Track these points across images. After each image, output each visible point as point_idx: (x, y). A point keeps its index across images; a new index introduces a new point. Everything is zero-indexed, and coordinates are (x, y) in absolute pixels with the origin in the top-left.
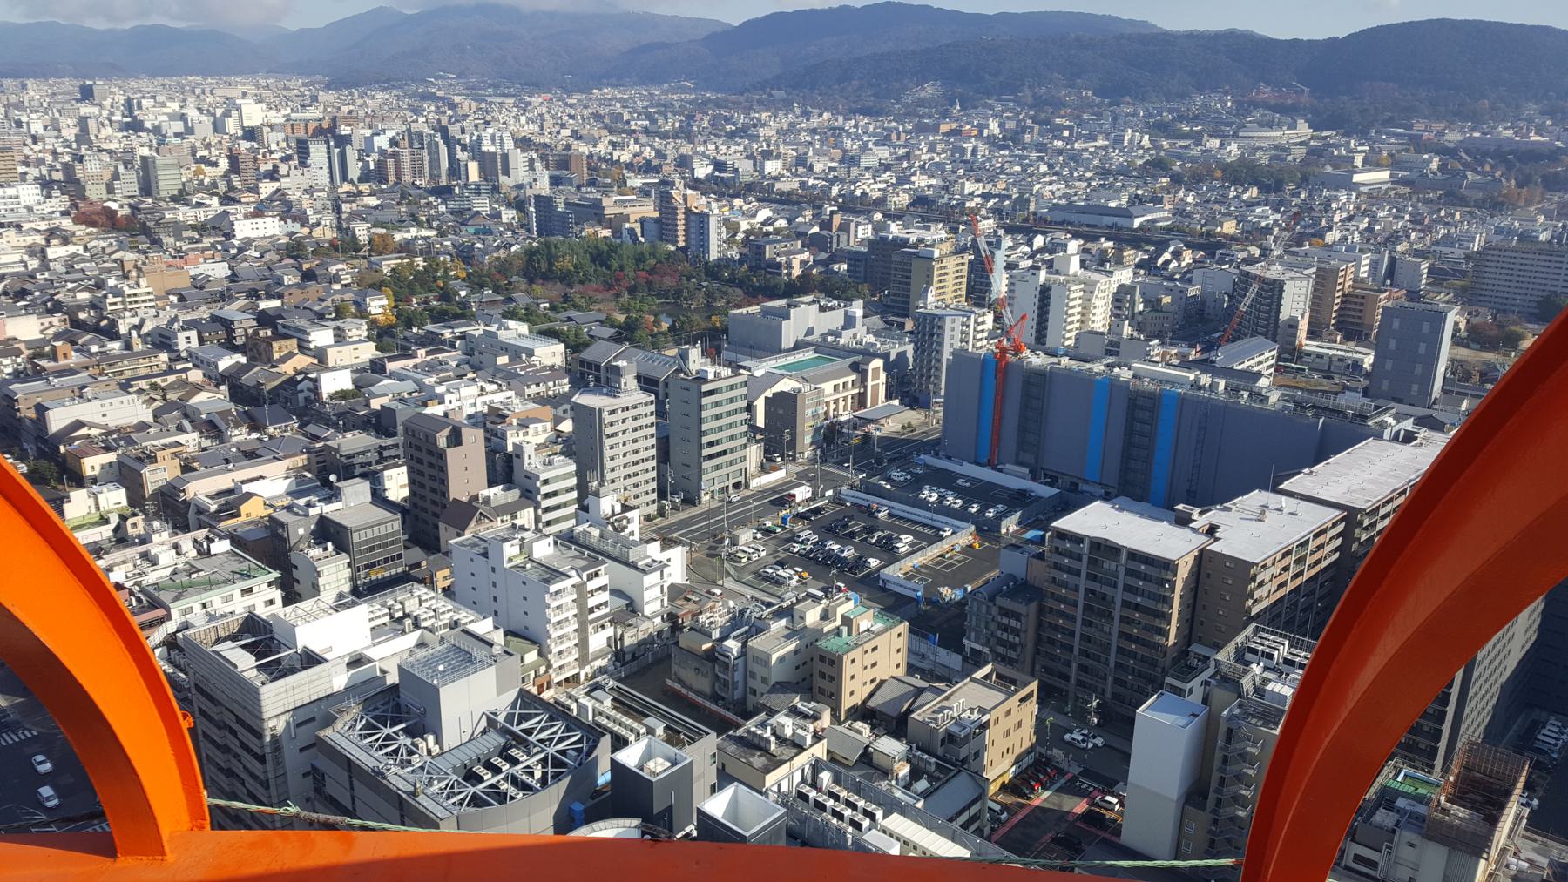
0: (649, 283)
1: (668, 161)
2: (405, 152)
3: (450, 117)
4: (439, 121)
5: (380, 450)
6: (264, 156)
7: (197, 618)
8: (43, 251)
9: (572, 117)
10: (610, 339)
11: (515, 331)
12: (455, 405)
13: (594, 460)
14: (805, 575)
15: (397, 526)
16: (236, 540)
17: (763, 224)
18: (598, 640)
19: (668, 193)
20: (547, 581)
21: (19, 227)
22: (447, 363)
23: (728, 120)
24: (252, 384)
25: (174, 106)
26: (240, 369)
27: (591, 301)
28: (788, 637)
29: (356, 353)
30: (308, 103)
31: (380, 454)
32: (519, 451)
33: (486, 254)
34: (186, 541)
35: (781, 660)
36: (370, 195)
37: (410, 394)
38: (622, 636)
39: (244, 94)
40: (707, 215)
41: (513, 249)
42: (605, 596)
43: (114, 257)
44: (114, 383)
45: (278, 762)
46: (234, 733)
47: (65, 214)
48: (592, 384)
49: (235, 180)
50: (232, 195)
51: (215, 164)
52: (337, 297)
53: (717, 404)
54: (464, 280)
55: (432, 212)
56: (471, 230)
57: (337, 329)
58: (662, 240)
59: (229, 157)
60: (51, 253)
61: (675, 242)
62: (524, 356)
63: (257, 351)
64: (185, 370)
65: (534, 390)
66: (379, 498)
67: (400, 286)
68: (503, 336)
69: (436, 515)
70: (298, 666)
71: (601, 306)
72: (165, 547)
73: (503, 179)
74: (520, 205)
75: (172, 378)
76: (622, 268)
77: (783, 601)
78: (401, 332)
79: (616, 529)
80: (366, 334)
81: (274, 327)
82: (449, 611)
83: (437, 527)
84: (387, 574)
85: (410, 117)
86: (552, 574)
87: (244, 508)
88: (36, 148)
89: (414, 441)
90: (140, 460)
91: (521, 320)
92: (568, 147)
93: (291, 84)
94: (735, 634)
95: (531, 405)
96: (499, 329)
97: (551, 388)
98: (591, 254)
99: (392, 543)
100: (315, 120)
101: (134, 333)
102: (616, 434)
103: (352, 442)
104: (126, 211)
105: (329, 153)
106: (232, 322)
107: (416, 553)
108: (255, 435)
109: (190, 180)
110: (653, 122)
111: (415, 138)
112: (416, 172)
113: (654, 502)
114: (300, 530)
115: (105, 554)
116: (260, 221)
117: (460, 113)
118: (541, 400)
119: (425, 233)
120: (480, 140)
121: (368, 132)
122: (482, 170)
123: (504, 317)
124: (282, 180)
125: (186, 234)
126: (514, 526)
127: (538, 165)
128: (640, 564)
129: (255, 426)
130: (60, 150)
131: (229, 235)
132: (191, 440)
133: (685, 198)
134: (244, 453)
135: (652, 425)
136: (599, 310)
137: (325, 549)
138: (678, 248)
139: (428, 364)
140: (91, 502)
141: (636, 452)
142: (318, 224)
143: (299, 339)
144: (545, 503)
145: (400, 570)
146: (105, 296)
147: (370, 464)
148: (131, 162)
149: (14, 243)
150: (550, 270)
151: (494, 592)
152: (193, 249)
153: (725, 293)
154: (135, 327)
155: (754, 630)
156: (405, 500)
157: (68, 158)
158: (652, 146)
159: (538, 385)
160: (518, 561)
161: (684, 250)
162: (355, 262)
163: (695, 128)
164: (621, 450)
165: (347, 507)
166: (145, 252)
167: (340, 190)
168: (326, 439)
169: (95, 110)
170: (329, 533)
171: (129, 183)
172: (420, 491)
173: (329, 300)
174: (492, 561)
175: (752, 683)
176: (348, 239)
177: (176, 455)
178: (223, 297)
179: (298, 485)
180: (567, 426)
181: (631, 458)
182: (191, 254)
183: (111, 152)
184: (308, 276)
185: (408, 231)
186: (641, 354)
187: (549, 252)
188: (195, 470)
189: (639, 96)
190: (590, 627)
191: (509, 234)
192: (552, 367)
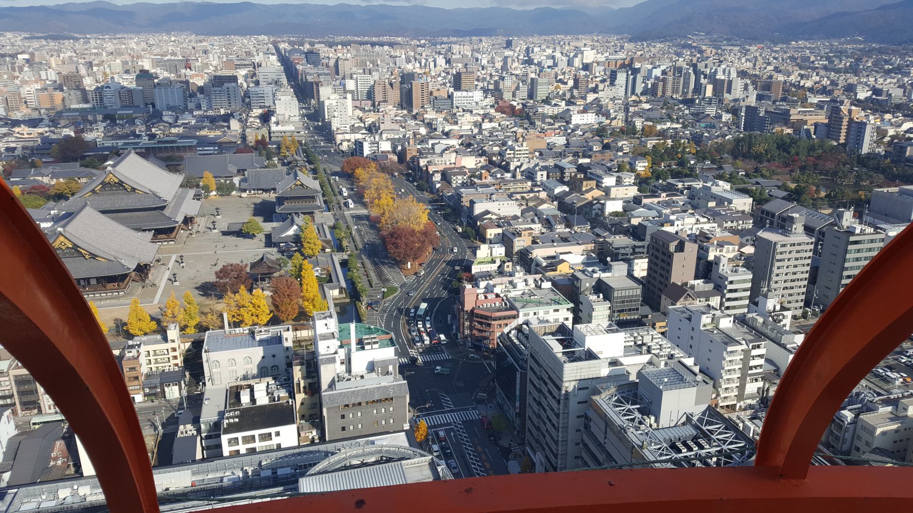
0: (815, 166)
1: (839, 87)
2: (670, 78)
3: (699, 58)
4: (691, 60)
5: (634, 247)
6: (592, 79)
7: (532, 318)
8: (481, 125)
9: (775, 58)
10: (783, 198)
11: (722, 187)
12: (680, 227)
13: (765, 274)
14: (909, 380)
15: (639, 292)
16: (554, 284)
17: (906, 132)
18: (752, 388)
19: (837, 107)
20: (726, 344)
21: (471, 112)
22: (677, 203)
23: (887, 62)
24: (570, 202)
25: (549, 51)
26: (565, 194)
27: (773, 173)
28: (892, 420)
29: (626, 192)
30: (618, 50)
31: (634, 250)
32: (717, 260)
33: (710, 140)
34: (531, 279)
35: (884, 433)
36: (645, 103)
37: (653, 218)
38: (768, 389)
39: (585, 45)
40: (865, 124)
41: (727, 138)
42: (761, 361)
43: (512, 130)
44: (505, 194)
45: (566, 406)
46: (546, 384)
47: (492, 106)
48: (768, 226)
49: (575, 92)
50: (572, 100)
51: (566, 83)
52: (620, 159)
53: (859, 251)
54: (694, 154)
55: (680, 113)
56: (703, 125)
57: (618, 177)
58: (828, 137)
59: (574, 80)
60: (484, 126)
61: (837, 140)
62: (726, 203)
63: (575, 185)
64: (539, 191)
65: (729, 224)
66: (630, 275)
67: (656, 156)
68: (715, 189)
69: (660, 290)
70: (584, 357)
71: (779, 177)
72: (521, 280)
73: (726, 95)
74: (735, 111)
75: (532, 195)
76: (797, 154)
77: (891, 394)
78: (653, 182)
79: (774, 321)
80: (633, 181)
81: (585, 174)
82: (669, 348)
83: (660, 297)
84: (629, 318)
85: (675, 58)
86: (729, 340)
87: (560, 267)
88: (483, 72)
89: (656, 246)
90: (514, 234)
91: (726, 181)
92: (771, 77)
93: (610, 39)
94: (850, 407)
95: (727, 234)
96: (712, 185)
97: (741, 225)
98: (777, 144)
99: (635, 301)
100: (621, 59)
101: (518, 169)
102: (783, 260)
103: (620, 241)
104: (520, 107)
105: (627, 78)
106: (565, 169)
107: (646, 310)
108: (568, 230)
109: (553, 92)
110: (831, 62)
111: (679, 70)
112: (675, 90)
113: (801, 308)
114: (587, 284)
115: (494, 278)
116: (585, 115)
117: (705, 55)
118: (733, 231)
119: (675, 126)
120: (716, 72)
121: (650, 67)
122: (714, 89)
123: (717, 179)
124: (600, 93)
125: (548, 120)
126: (709, 305)
127: (751, 88)
128: (788, 346)
129: (569, 225)
130: (493, 74)
131: (568, 122)
132: (537, 227)
133: (850, 111)
134: (562, 238)
135: (809, 258)
136: (778, 179)
137: (599, 297)
138: (839, 144)
139: (666, 202)
140: (489, 251)
141: (795, 273)
142: (615, 118)
143: (597, 181)
144: (728, 295)
145: (636, 317)
146: (506, 150)
147: (627, 254)
148: (525, 81)
149: (469, 120)
150: (749, 152)
151: (691, 342)
152: (549, 129)
153: (871, 176)
154: (518, 167)
155: (865, 408)
156: (643, 278)
157: (497, 78)
158: (828, 78)
159: (732, 222)
160: (709, 327)
161: (844, 145)
162: (633, 140)
163: (861, 67)
164: (785, 270)
165: (613, 276)
166: (526, 129)
167: (630, 99)
168: (604, 237)
169: (511, 53)
170: (601, 288)
171: (523, 92)
172: (653, 274)
173: (616, 161)
174: (693, 324)
175: (857, 443)
176: (631, 127)
177: (530, 234)
178: (562, 155)
179: (588, 259)
180: (749, 250)
181: (790, 277)
182: (549, 131)
183: (517, 75)
184: (606, 147)
185: (666, 124)
186: (805, 211)
187: (749, 141)
188: (537, 243)
189: (823, 46)
190: (748, 378)
191: (726, 128)
192: (743, 212)
